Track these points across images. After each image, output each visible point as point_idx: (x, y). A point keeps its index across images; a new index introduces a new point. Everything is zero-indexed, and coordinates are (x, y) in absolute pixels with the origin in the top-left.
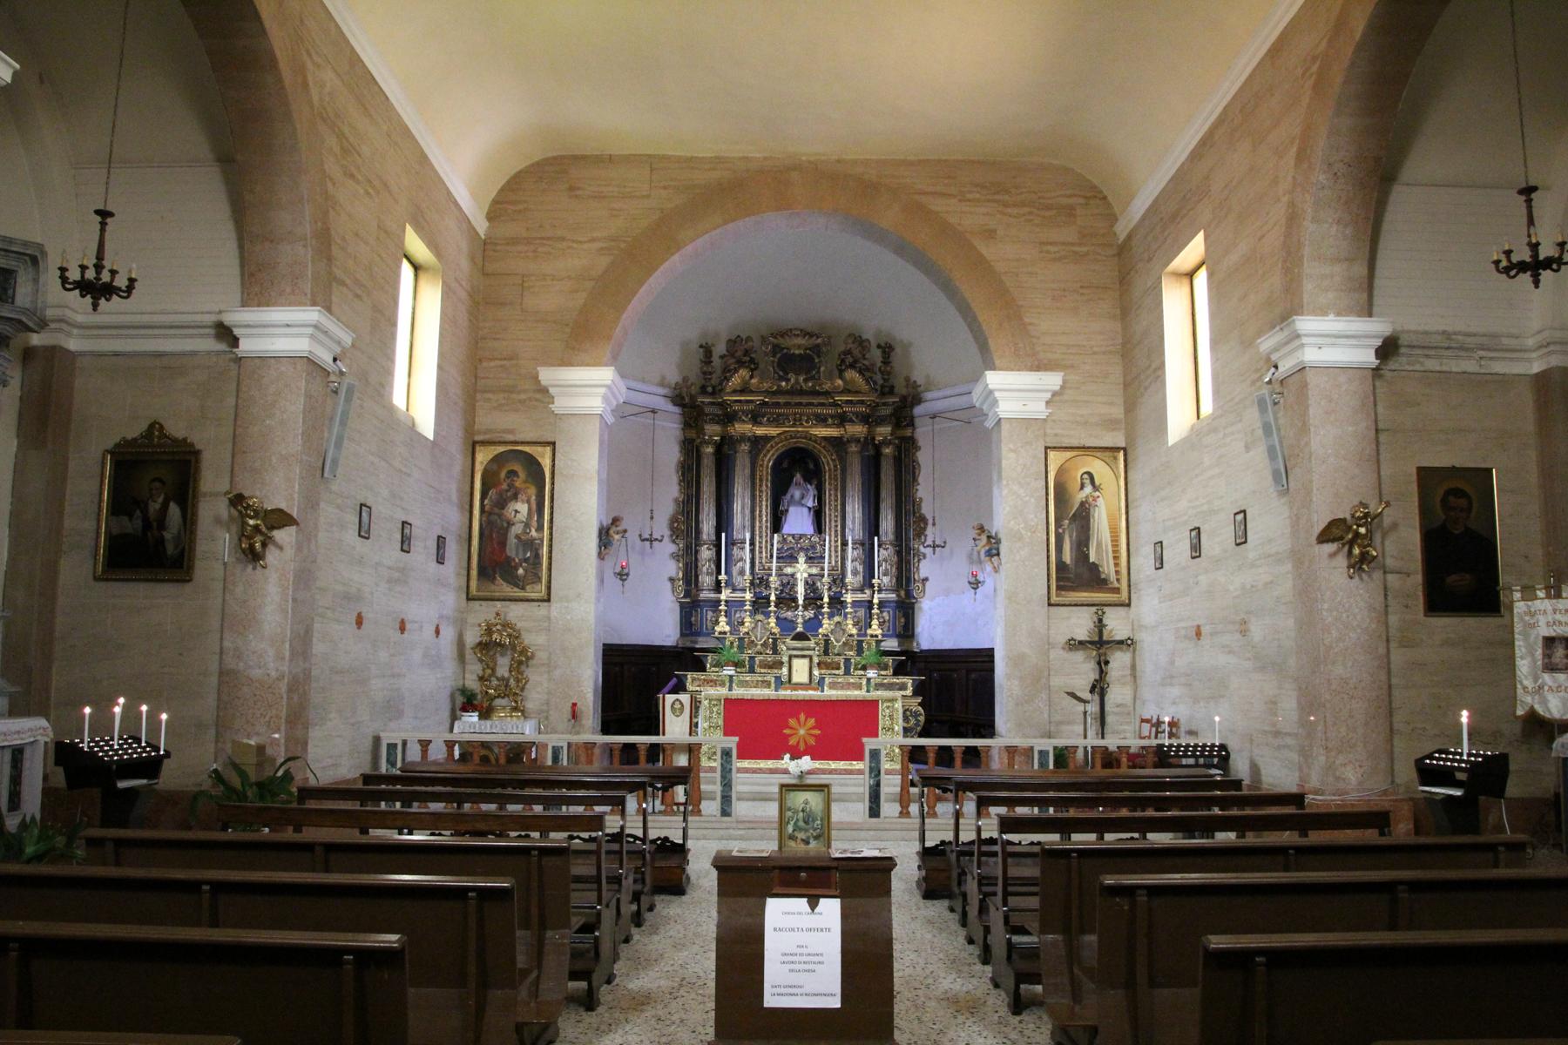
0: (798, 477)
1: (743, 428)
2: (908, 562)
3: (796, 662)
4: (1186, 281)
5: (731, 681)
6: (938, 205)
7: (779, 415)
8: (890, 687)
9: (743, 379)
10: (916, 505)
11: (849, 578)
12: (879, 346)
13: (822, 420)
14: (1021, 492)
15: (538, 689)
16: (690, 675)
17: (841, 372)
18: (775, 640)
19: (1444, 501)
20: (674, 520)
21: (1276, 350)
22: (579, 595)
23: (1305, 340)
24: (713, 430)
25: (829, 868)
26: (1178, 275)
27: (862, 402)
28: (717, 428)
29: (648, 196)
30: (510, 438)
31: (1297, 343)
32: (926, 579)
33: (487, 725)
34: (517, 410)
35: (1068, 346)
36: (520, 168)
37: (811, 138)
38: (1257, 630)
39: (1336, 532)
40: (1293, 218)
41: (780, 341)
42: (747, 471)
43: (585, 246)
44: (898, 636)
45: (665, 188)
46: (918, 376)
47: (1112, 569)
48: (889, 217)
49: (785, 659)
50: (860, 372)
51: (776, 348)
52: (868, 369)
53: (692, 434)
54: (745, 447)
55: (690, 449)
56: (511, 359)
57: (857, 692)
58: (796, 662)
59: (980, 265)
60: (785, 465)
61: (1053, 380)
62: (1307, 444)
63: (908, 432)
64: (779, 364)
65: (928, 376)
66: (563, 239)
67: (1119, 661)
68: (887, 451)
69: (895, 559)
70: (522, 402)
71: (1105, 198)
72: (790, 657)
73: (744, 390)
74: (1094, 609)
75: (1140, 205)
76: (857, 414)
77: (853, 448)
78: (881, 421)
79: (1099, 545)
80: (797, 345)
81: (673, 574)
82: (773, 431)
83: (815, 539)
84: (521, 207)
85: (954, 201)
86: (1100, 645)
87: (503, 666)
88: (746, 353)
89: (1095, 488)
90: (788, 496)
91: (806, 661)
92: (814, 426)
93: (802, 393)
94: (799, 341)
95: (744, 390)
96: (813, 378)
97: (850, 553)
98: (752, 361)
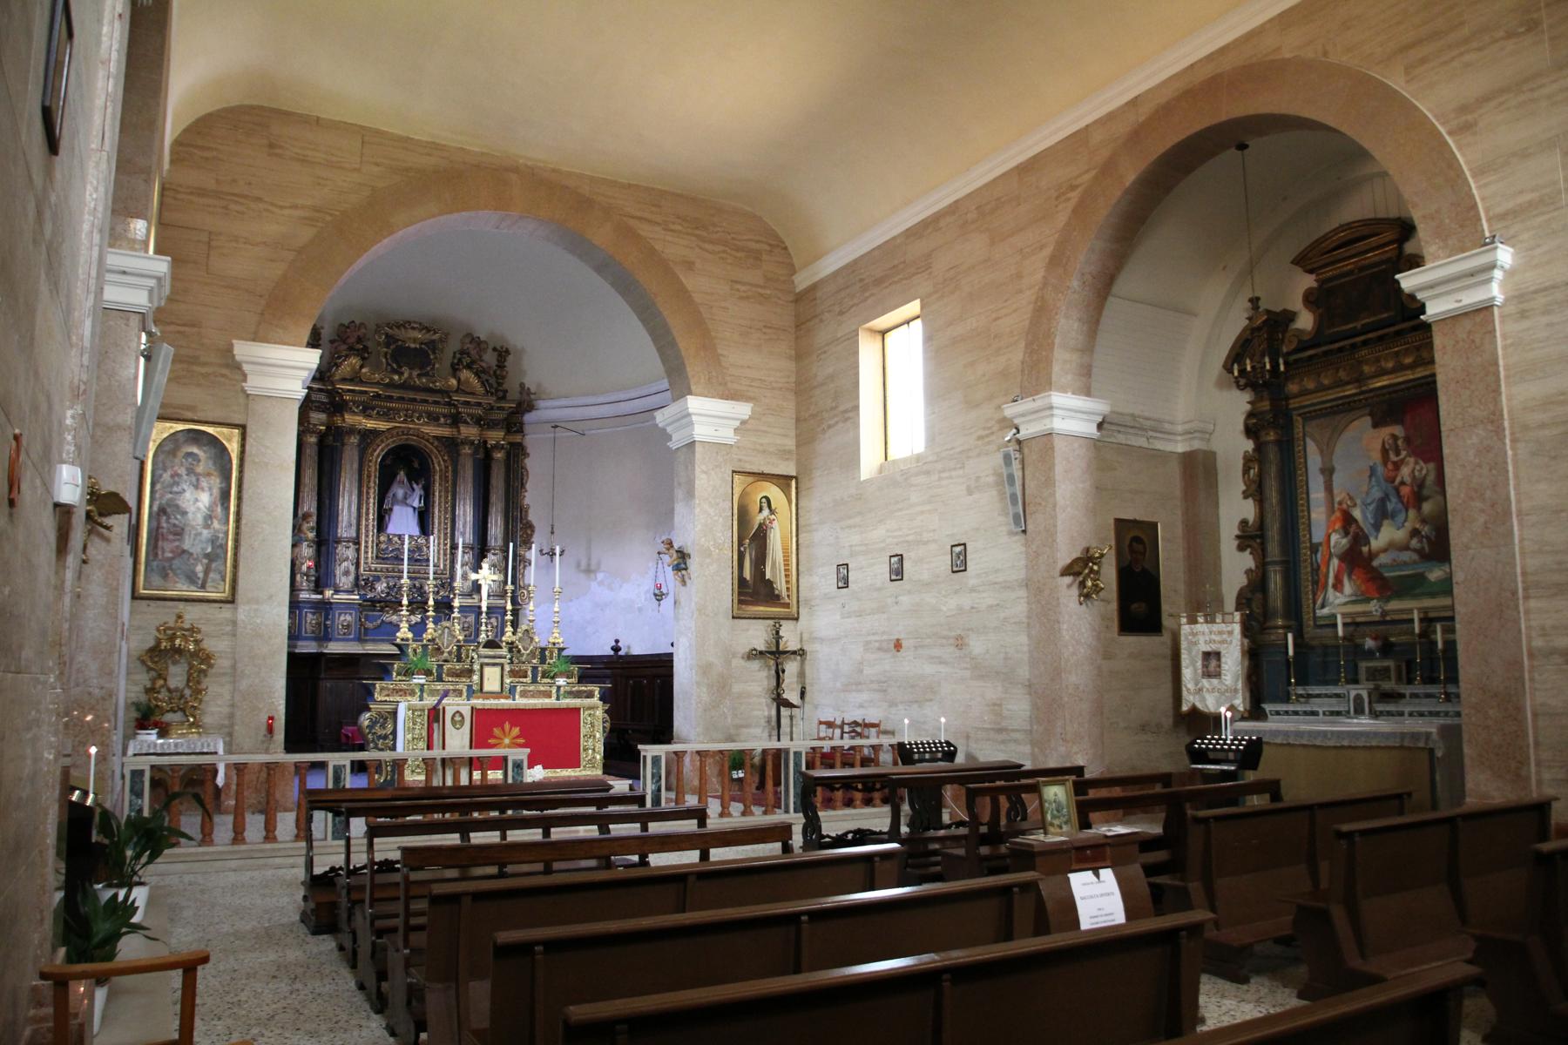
0: (402, 475)
1: (350, 419)
3: (487, 670)
4: (879, 338)
5: (422, 691)
6: (645, 230)
7: (390, 409)
8: (578, 695)
10: (523, 511)
13: (433, 418)
14: (711, 511)
15: (217, 700)
16: (378, 684)
18: (459, 647)
19: (1130, 545)
21: (1023, 415)
22: (271, 597)
23: (1056, 412)
25: (1103, 845)
26: (873, 331)
27: (479, 404)
28: (323, 416)
29: (358, 170)
30: (189, 415)
31: (1048, 413)
33: (171, 742)
34: (199, 385)
35: (753, 380)
36: (210, 110)
37: (538, 145)
38: (977, 646)
39: (1077, 568)
40: (1042, 311)
41: (396, 332)
42: (356, 466)
43: (286, 212)
45: (377, 164)
46: (530, 383)
47: (784, 586)
48: (602, 236)
49: (476, 667)
50: (476, 374)
52: (484, 371)
54: (354, 440)
56: (193, 326)
57: (547, 700)
58: (487, 670)
59: (683, 294)
61: (744, 410)
62: (1053, 494)
63: (518, 439)
64: (393, 356)
65: (539, 385)
66: (259, 199)
67: (791, 667)
68: (499, 455)
70: (205, 376)
71: (786, 248)
72: (482, 666)
73: (355, 378)
74: (771, 622)
75: (830, 264)
76: (471, 416)
77: (467, 450)
78: (492, 425)
79: (774, 563)
82: (382, 426)
84: (206, 154)
85: (657, 229)
86: (775, 655)
87: (177, 676)
88: (359, 340)
89: (772, 512)
91: (498, 669)
95: (355, 378)
96: (426, 375)
98: (366, 349)
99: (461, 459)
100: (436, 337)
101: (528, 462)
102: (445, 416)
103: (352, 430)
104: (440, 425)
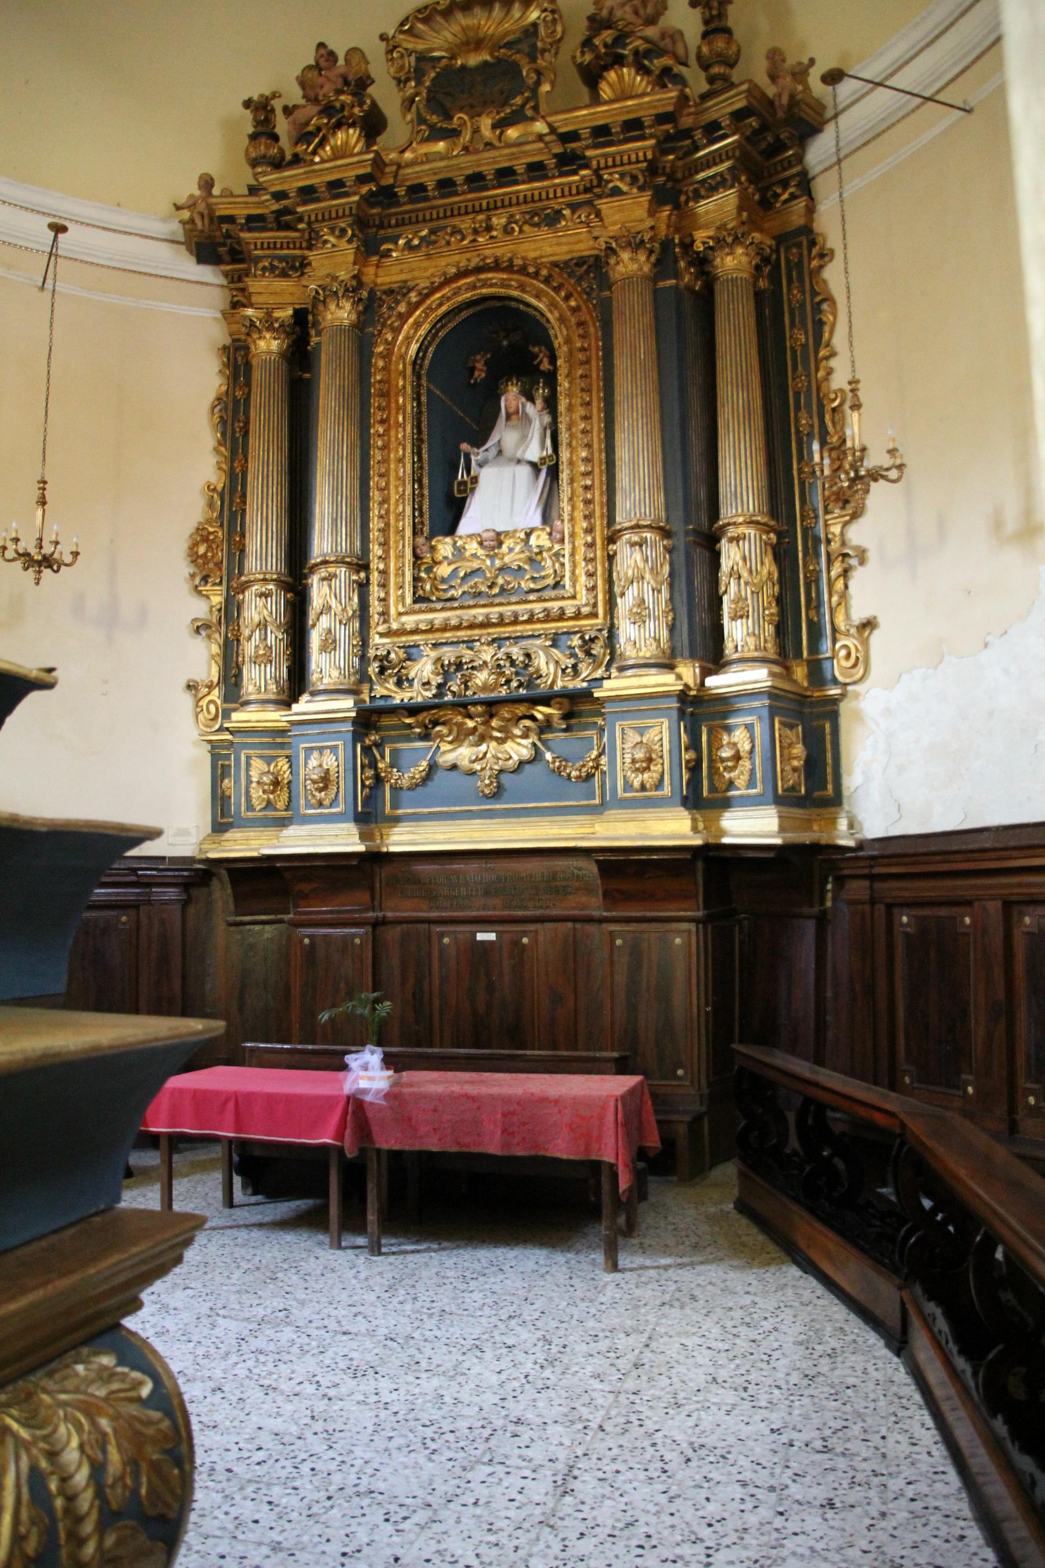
2: (813, 580)
11: (627, 630)
32: (868, 625)
44: (784, 800)
55: (237, 360)
60: (480, 374)
69: (768, 567)
97: (629, 559)
101: (832, 275)
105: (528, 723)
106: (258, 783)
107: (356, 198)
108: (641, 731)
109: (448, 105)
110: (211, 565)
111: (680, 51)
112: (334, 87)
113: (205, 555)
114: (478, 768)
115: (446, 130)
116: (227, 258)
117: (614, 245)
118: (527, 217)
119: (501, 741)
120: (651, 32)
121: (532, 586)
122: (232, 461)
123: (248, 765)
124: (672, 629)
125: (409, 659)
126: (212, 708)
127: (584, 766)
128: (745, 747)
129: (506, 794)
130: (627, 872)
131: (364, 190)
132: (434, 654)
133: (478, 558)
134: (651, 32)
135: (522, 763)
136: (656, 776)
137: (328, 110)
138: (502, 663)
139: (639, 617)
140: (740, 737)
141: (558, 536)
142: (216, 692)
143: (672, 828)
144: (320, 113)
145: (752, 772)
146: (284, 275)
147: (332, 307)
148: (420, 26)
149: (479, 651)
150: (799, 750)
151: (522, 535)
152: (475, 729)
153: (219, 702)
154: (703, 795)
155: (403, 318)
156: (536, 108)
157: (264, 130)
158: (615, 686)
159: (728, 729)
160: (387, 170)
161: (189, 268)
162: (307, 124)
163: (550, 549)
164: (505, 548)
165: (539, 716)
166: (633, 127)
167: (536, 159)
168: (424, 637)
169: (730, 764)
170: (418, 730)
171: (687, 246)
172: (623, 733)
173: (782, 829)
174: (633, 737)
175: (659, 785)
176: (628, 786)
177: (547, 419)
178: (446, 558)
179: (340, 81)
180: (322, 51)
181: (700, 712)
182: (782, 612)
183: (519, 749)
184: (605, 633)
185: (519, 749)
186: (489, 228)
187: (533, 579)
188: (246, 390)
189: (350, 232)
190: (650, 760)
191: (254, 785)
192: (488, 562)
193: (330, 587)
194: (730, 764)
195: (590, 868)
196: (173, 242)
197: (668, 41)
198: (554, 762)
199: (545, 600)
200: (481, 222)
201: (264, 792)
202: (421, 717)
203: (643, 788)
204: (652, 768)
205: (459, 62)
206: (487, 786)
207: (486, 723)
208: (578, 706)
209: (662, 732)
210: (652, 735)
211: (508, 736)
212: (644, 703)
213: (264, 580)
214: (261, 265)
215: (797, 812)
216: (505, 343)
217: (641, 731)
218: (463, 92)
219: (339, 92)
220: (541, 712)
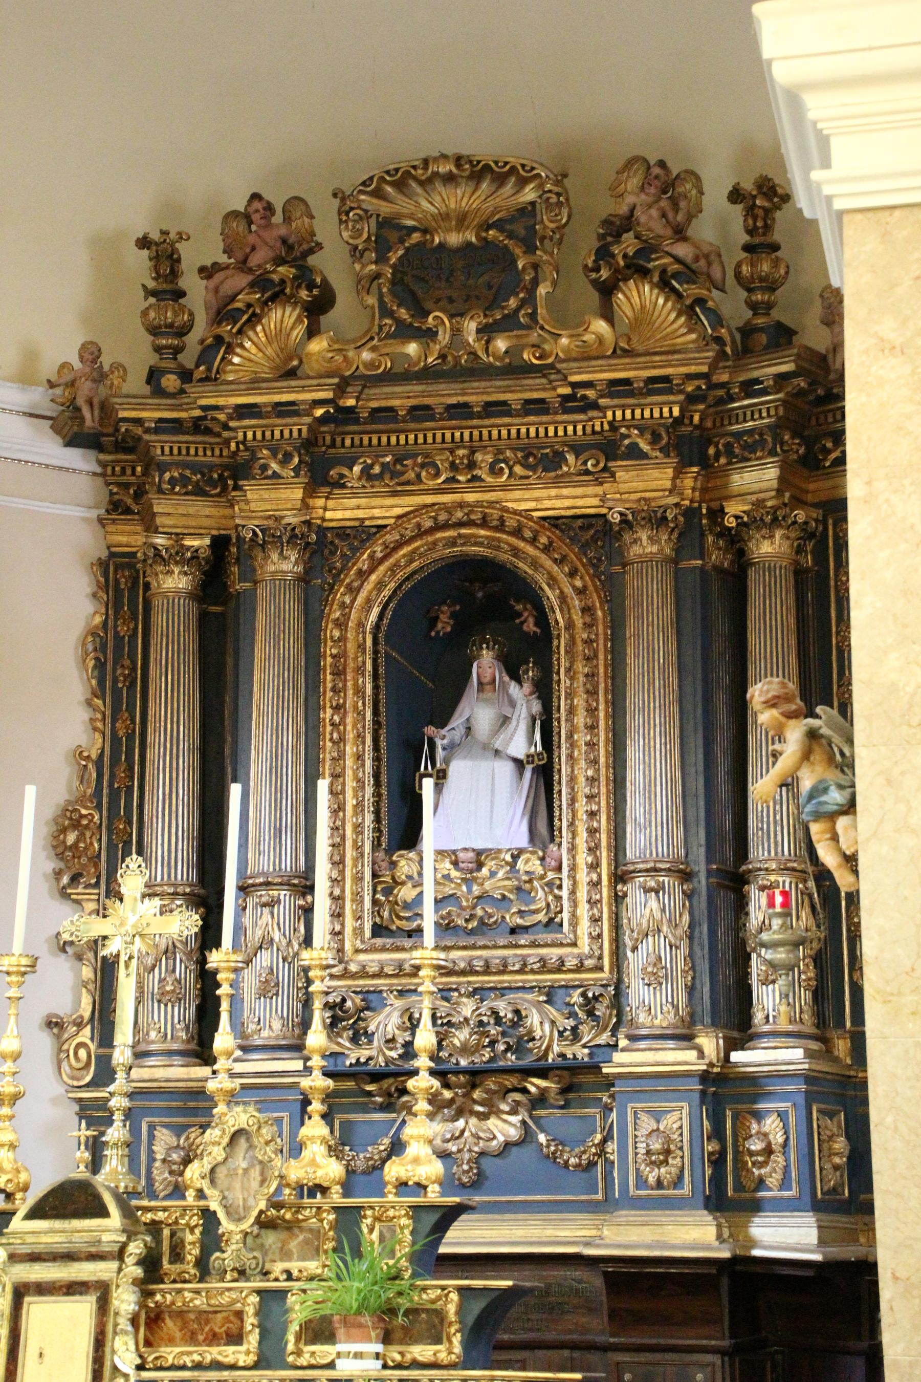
0: (486, 663)
1: (276, 499)
9: (281, 333)
11: (638, 993)
12: (736, 195)
13: (545, 461)
17: (607, 290)
20: (68, 820)
24: (186, 520)
42: (292, 646)
50: (664, 284)
51: (388, 230)
52: (689, 273)
53: (130, 537)
54: (284, 564)
55: (122, 583)
60: (444, 625)
68: (769, 548)
77: (645, 545)
78: (748, 449)
80: (449, 213)
81: (62, 1007)
82: (383, 509)
83: (530, 864)
90: (457, 721)
91: (83, 1308)
92: (523, 483)
93: (477, 371)
94: (458, 198)
96: (508, 324)
97: (643, 907)
99: (632, 583)
100: (529, 194)
102: (577, 449)
103: (272, 537)
104: (557, 482)
105: (517, 1096)
106: (164, 1161)
107: (308, 420)
108: (657, 1116)
109: (420, 293)
110: (84, 860)
111: (716, 273)
112: (271, 254)
113: (75, 845)
114: (454, 1149)
115: (419, 329)
116: (111, 448)
117: (630, 517)
118: (520, 454)
119: (483, 1117)
120: (682, 250)
121: (519, 921)
122: (114, 721)
123: (151, 1137)
124: (691, 990)
125: (367, 1008)
126: (82, 1053)
127: (584, 1152)
128: (778, 1138)
129: (487, 1183)
130: (640, 1287)
131: (319, 412)
132: (399, 1003)
133: (451, 881)
134: (682, 250)
135: (507, 1145)
136: (674, 1170)
137: (261, 283)
138: (485, 1019)
139: (654, 980)
140: (771, 1124)
141: (553, 863)
142: (87, 1031)
143: (693, 1235)
144: (252, 285)
145: (786, 1169)
146: (199, 492)
147: (275, 557)
148: (389, 189)
149: (458, 1003)
150: (840, 1144)
151: (508, 858)
152: (452, 1100)
153: (92, 1047)
154: (729, 1194)
155: (363, 575)
156: (533, 316)
157: (167, 289)
158: (626, 1060)
159: (758, 1116)
160: (349, 389)
161: (54, 451)
162: (233, 298)
163: (542, 877)
164: (485, 871)
165: (533, 1089)
166: (659, 385)
167: (536, 395)
168: (387, 981)
169: (760, 1159)
170: (379, 1099)
171: (717, 514)
172: (636, 1118)
173: (822, 1242)
174: (647, 1124)
175: (678, 1182)
176: (641, 1182)
177: (536, 707)
178: (410, 877)
179: (279, 244)
180: (257, 205)
181: (725, 1095)
182: (821, 976)
183: (504, 1128)
184: (611, 989)
185: (504, 1128)
186: (472, 465)
187: (520, 912)
188: (132, 626)
189: (296, 460)
190: (667, 1152)
191: (157, 1164)
192: (464, 888)
193: (272, 914)
194: (760, 1159)
195: (596, 1281)
196: (31, 415)
197: (702, 263)
198: (548, 1146)
199: (539, 946)
200: (462, 458)
201: (171, 1173)
202: (385, 1083)
203: (659, 1184)
204: (670, 1161)
205: (437, 240)
206: (464, 1172)
207: (467, 1095)
208: (580, 1081)
209: (679, 1118)
210: (670, 1122)
211: (493, 1111)
212: (663, 1082)
213: (175, 894)
214: (167, 476)
215: (842, 1220)
216: (480, 594)
217: (657, 1116)
218: (439, 278)
219: (279, 261)
220: (535, 1084)
